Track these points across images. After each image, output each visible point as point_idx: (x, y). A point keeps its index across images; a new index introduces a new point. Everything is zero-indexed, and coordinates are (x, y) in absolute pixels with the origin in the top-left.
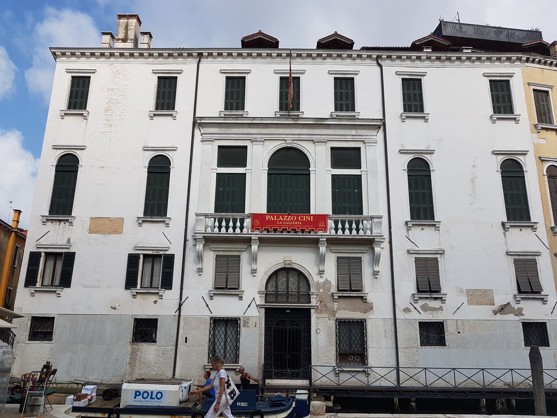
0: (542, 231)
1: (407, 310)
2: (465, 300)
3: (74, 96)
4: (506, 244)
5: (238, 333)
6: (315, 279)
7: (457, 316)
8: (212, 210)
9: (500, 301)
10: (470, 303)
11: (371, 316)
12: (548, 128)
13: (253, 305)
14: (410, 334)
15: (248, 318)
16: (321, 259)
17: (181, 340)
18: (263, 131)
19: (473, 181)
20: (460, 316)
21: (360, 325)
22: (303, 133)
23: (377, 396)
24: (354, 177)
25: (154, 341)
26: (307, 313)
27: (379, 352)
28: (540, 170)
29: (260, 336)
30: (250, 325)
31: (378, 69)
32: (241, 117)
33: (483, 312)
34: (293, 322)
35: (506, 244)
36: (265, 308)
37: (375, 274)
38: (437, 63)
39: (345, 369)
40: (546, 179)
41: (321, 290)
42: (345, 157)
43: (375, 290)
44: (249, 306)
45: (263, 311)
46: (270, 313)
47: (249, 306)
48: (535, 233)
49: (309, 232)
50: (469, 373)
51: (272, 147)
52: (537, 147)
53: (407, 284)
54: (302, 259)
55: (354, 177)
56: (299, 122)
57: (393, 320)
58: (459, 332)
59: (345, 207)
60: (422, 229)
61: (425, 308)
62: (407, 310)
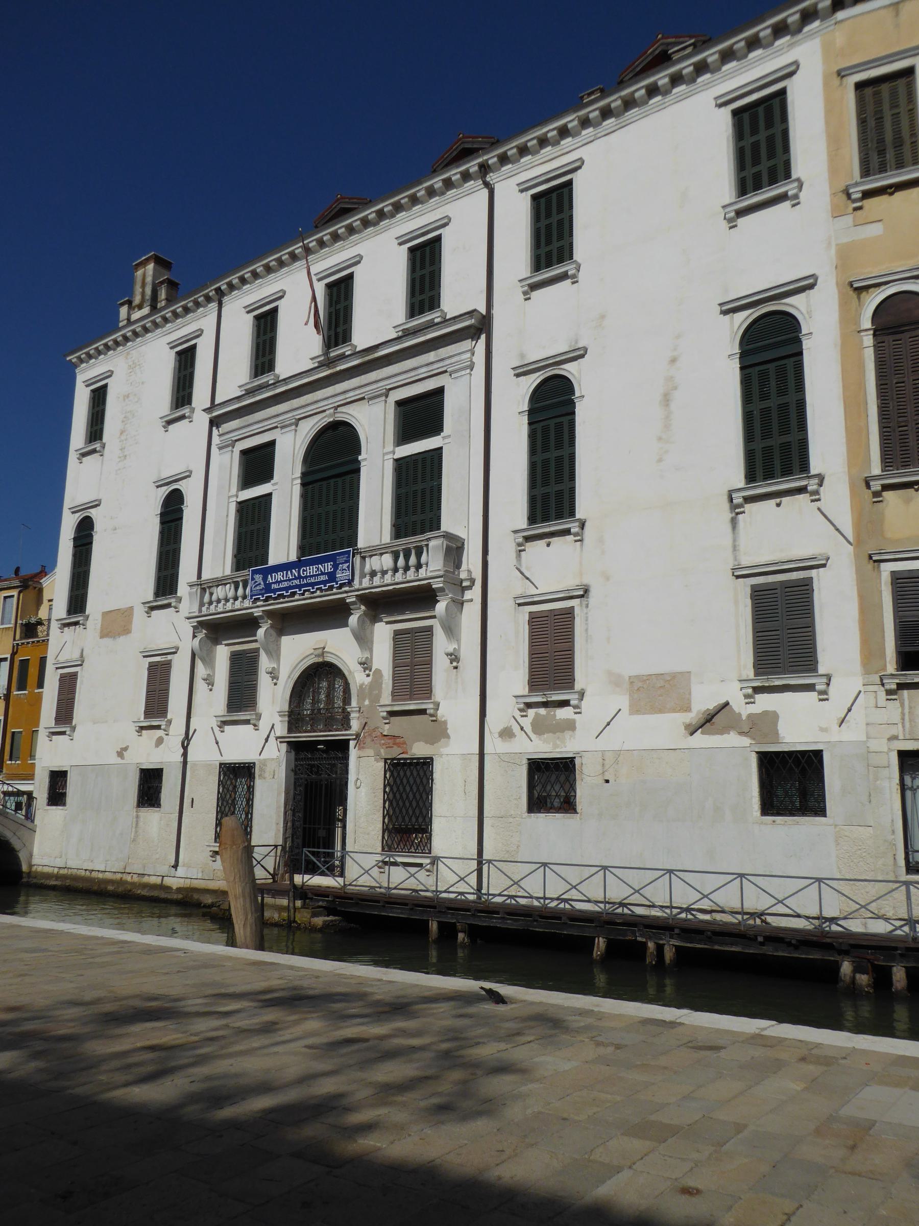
0: (838, 496)
1: (506, 734)
2: (623, 701)
3: (261, 353)
4: (735, 548)
5: (251, 790)
6: (358, 678)
7: (603, 744)
8: (387, 538)
9: (704, 700)
10: (636, 709)
11: (444, 751)
12: (890, 186)
13: (272, 739)
14: (510, 787)
15: (264, 763)
16: (363, 639)
17: (187, 802)
18: (296, 403)
19: (666, 400)
20: (612, 741)
21: (425, 765)
22: (319, 398)
23: (402, 913)
24: (252, 502)
25: (159, 806)
26: (342, 747)
27: (450, 829)
28: (848, 319)
29: (279, 794)
30: (267, 775)
31: (485, 192)
32: (278, 382)
33: (665, 730)
34: (312, 766)
35: (735, 548)
36: (288, 742)
37: (454, 658)
38: (588, 132)
39: (399, 860)
40: (868, 340)
41: (367, 702)
42: (421, 415)
43: (452, 697)
44: (217, 743)
45: (284, 747)
46: (296, 748)
47: (217, 743)
48: (817, 504)
49: (303, 594)
50: (636, 879)
51: (308, 429)
52: (845, 255)
53: (511, 675)
54: (337, 644)
55: (252, 502)
56: (338, 369)
57: (476, 759)
58: (607, 781)
59: (414, 523)
60: (778, 505)
61: (539, 728)
62: (506, 734)
